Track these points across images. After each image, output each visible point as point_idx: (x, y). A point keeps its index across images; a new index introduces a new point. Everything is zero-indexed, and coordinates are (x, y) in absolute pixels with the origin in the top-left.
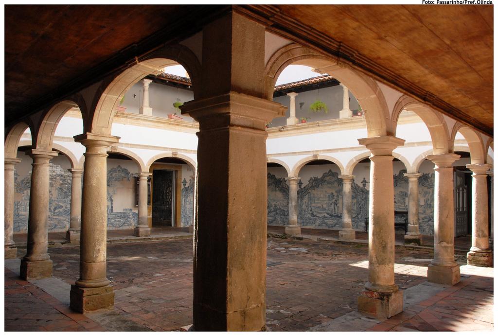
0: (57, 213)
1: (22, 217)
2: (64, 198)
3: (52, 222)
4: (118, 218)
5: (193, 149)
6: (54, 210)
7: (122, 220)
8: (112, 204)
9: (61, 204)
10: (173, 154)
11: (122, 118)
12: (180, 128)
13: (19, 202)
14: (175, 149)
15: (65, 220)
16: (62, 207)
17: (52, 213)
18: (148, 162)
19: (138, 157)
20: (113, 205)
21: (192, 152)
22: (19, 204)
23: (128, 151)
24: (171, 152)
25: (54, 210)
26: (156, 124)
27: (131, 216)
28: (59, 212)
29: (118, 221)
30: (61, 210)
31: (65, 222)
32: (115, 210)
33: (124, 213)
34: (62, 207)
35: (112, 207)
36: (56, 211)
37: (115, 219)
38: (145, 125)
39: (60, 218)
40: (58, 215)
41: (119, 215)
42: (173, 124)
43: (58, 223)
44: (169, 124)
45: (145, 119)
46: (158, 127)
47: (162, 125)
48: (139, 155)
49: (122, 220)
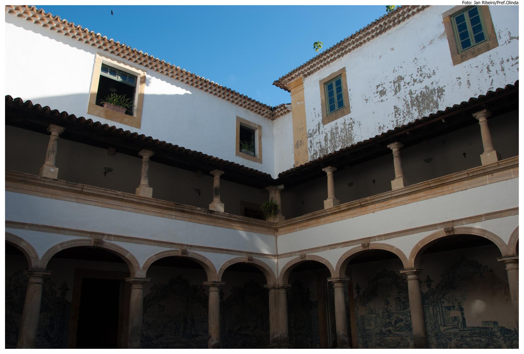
0: (398, 328)
1: (368, 332)
2: (403, 310)
3: (395, 339)
4: (476, 335)
5: (482, 214)
6: (395, 324)
7: (483, 340)
8: (463, 314)
9: (401, 317)
10: (447, 231)
11: (369, 206)
12: (450, 187)
13: (364, 315)
14: (449, 222)
15: (407, 337)
16: (402, 320)
17: (394, 328)
18: (411, 253)
19: (397, 249)
20: (466, 316)
21: (483, 218)
22: (364, 318)
23: (383, 244)
24: (443, 229)
25: (395, 324)
26: (413, 196)
27: (498, 334)
28: (400, 326)
29: (478, 340)
30: (402, 324)
31: (408, 338)
32: (469, 324)
33: (484, 328)
34: (402, 320)
35: (464, 319)
36: (397, 326)
37: (472, 337)
38: (397, 204)
39: (402, 333)
40: (399, 331)
41: (477, 331)
42: (437, 187)
43: (401, 340)
44: (431, 188)
45: (393, 196)
46: (416, 199)
47: (421, 194)
48: (397, 246)
49: (483, 340)
